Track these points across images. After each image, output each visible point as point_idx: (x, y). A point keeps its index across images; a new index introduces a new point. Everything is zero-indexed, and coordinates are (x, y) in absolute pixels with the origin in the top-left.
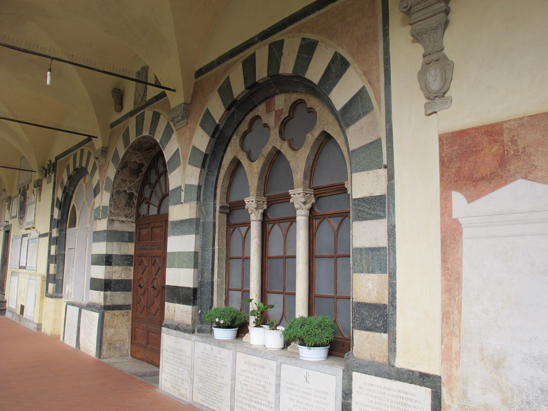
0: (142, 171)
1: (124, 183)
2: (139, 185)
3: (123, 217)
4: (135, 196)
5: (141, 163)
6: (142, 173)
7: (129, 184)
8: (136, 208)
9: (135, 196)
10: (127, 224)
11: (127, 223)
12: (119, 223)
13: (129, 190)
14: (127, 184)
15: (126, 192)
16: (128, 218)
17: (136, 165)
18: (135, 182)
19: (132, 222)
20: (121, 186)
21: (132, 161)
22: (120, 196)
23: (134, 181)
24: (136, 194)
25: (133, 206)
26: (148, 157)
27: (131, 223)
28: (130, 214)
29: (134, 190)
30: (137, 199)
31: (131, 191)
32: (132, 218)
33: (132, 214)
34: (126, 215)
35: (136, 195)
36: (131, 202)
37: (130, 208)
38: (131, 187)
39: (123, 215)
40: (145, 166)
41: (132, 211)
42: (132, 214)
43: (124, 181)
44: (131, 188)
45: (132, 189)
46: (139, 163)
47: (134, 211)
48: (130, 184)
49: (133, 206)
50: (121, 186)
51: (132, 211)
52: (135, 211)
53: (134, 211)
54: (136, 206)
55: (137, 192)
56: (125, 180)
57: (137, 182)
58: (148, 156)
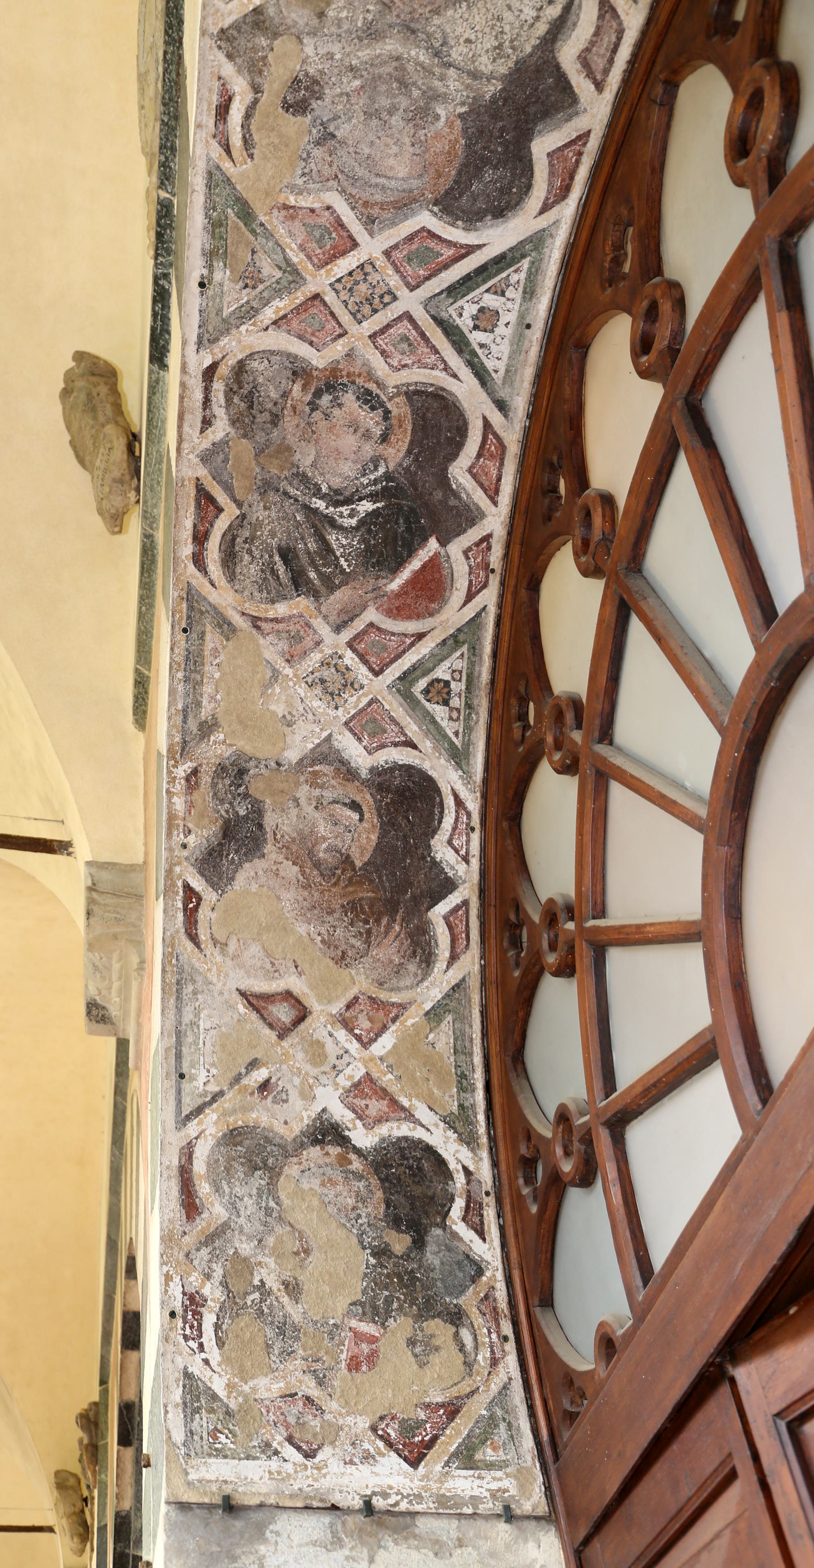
0: (448, 886)
1: (293, 1039)
2: (461, 1050)
3: (367, 1457)
4: (460, 1179)
5: (397, 767)
6: (453, 900)
7: (354, 1047)
8: (507, 1329)
9: (460, 1179)
10: (439, 1549)
11: (447, 1529)
12: (337, 1542)
13: (371, 1123)
14: (331, 1050)
15: (343, 1141)
16: (434, 1463)
17: (355, 806)
18: (412, 1018)
19: (509, 1515)
20: (260, 1075)
21: (292, 756)
22: (285, 1188)
23: (403, 1007)
24: (465, 1155)
25: (469, 1300)
26: (442, 672)
27: (502, 1527)
28: (452, 1410)
29: (422, 1112)
30: (490, 1214)
31: (404, 1130)
32: (488, 1454)
33: (478, 1408)
34: (409, 1428)
35: (465, 1169)
36: (432, 1256)
37: (439, 1328)
38: (387, 1079)
39: (363, 1423)
40: (450, 802)
41: (469, 1365)
42: (478, 1408)
43: (283, 1013)
44: (384, 1093)
45: (394, 1103)
46: (372, 770)
47: (494, 1362)
48: (365, 1044)
49: (469, 1300)
50: (260, 1075)
51: (469, 1365)
52: (512, 1360)
53: (494, 1362)
54: (502, 1303)
55: (469, 1140)
56: (288, 995)
57: (434, 1015)
58: (437, 659)
